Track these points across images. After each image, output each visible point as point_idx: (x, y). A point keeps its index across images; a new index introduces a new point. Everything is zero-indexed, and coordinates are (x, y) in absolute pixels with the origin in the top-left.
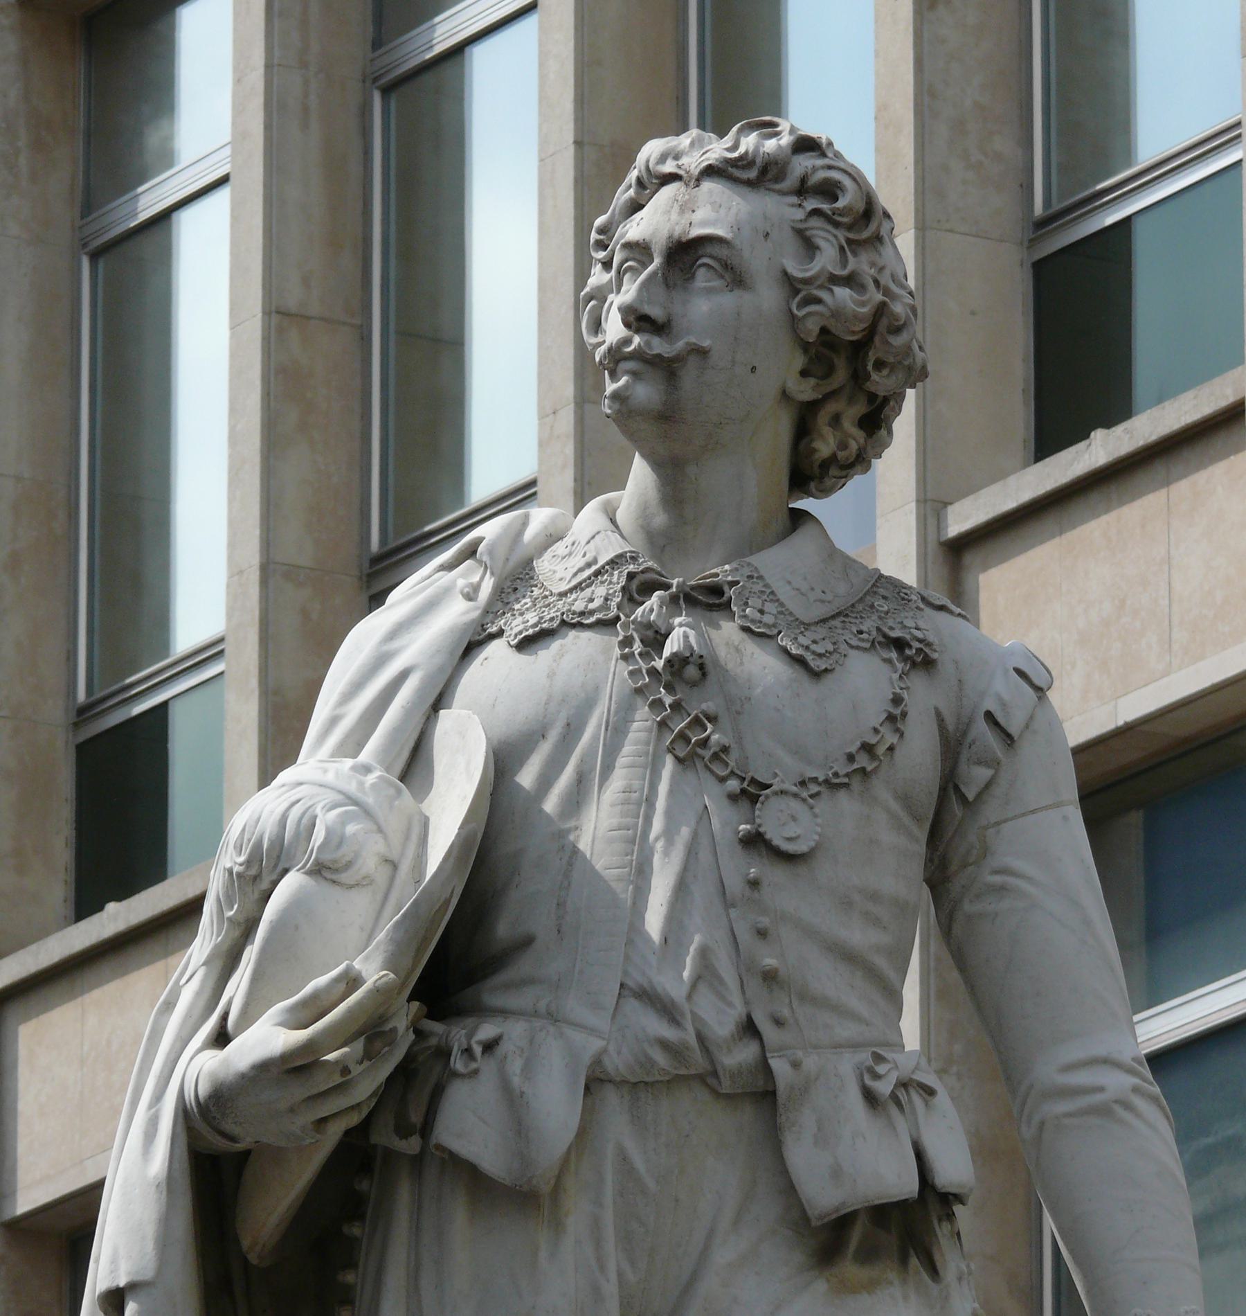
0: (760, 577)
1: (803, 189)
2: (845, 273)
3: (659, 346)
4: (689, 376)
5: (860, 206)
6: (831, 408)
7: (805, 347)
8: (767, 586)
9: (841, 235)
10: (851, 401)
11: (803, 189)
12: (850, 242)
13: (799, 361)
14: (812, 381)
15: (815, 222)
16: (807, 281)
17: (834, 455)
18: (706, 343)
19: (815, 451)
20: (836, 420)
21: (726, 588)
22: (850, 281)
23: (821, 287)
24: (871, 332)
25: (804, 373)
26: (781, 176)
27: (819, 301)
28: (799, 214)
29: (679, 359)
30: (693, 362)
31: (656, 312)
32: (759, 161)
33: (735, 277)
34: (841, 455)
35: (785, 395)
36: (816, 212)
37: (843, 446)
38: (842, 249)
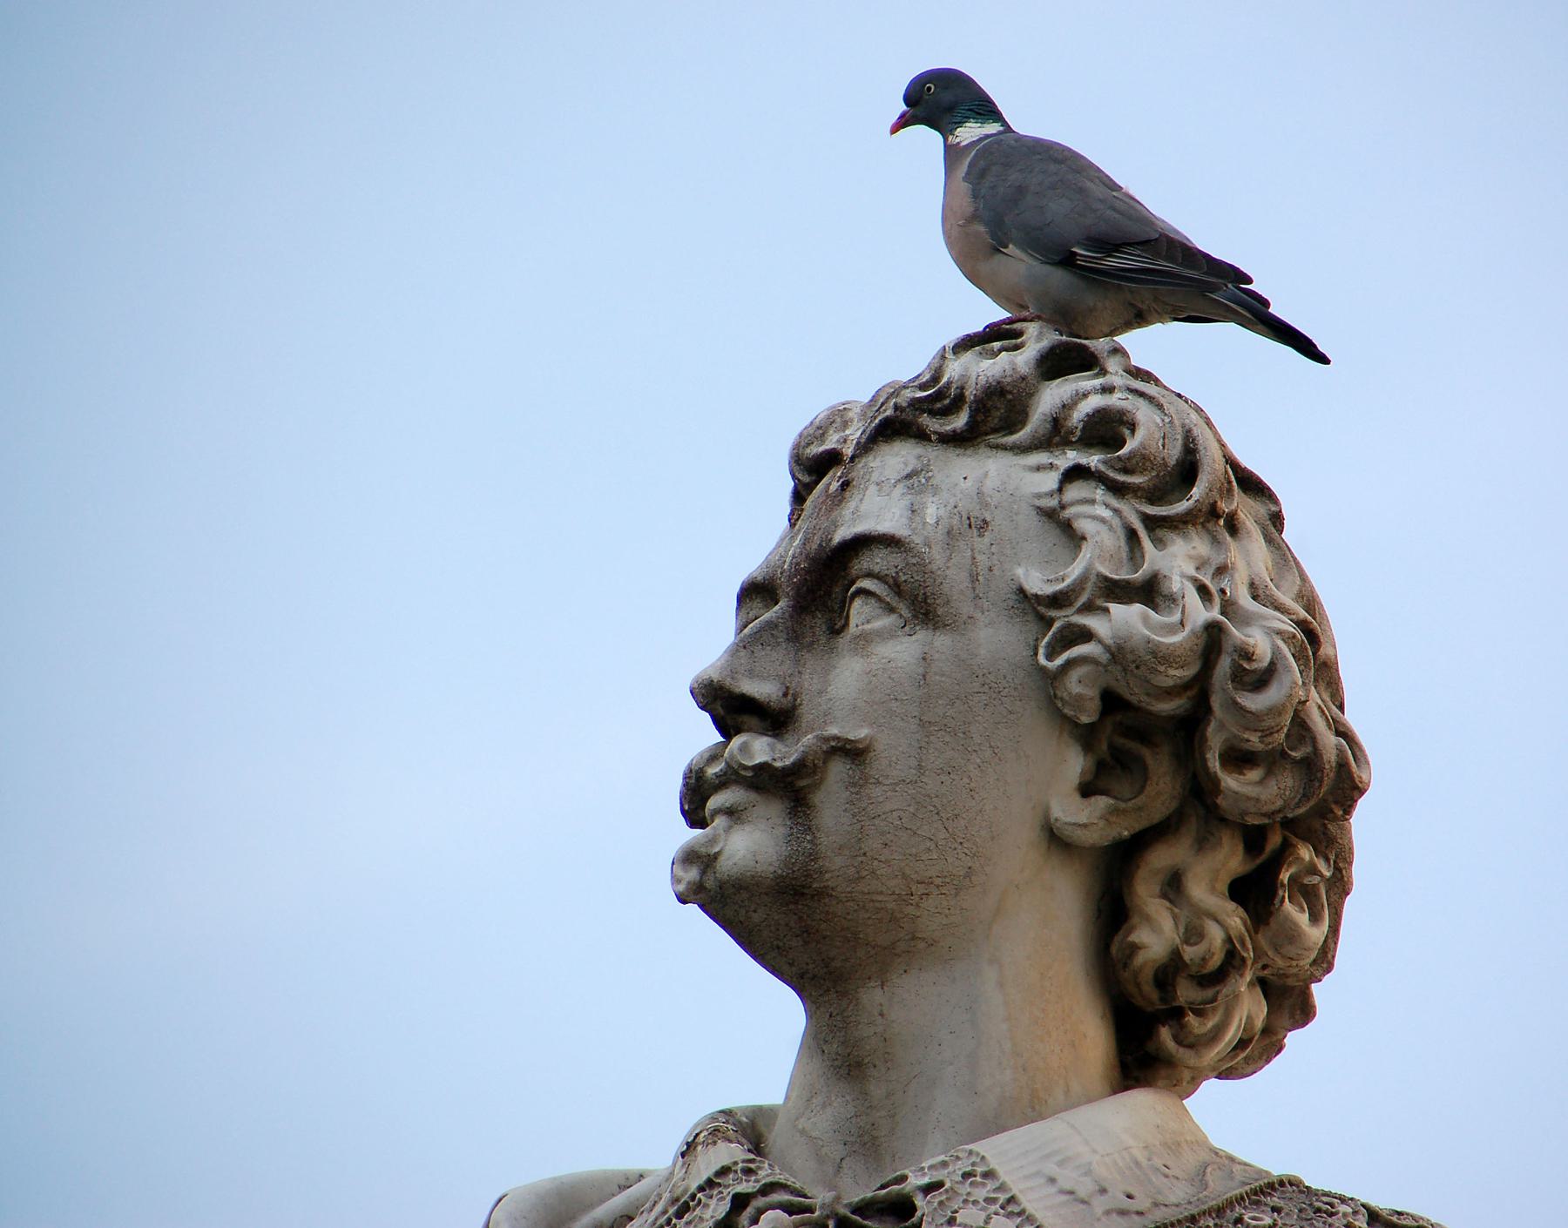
0: (989, 1175)
1: (1056, 435)
2: (1139, 576)
3: (759, 749)
4: (832, 800)
5: (1174, 453)
6: (1161, 858)
7: (1086, 737)
8: (1002, 1188)
9: (1131, 511)
10: (1202, 844)
11: (1056, 435)
12: (1152, 523)
13: (1075, 764)
14: (1102, 802)
15: (1075, 491)
16: (1058, 600)
17: (1176, 955)
18: (859, 733)
19: (1135, 948)
20: (1173, 886)
21: (919, 1201)
22: (1149, 592)
23: (1089, 608)
24: (1199, 687)
25: (1087, 790)
26: (1015, 416)
27: (1086, 635)
28: (1051, 481)
29: (800, 768)
30: (838, 770)
31: (762, 689)
32: (970, 394)
33: (921, 605)
34: (1189, 953)
35: (1055, 839)
36: (1076, 473)
37: (1193, 934)
38: (1132, 535)
